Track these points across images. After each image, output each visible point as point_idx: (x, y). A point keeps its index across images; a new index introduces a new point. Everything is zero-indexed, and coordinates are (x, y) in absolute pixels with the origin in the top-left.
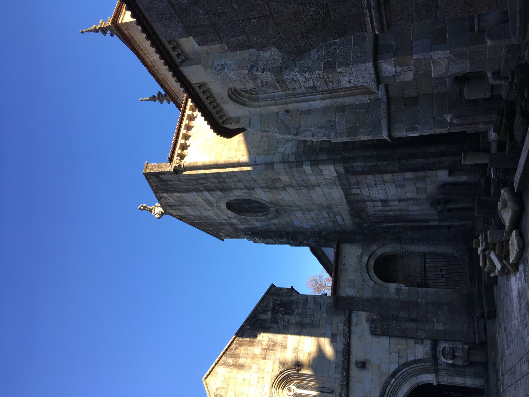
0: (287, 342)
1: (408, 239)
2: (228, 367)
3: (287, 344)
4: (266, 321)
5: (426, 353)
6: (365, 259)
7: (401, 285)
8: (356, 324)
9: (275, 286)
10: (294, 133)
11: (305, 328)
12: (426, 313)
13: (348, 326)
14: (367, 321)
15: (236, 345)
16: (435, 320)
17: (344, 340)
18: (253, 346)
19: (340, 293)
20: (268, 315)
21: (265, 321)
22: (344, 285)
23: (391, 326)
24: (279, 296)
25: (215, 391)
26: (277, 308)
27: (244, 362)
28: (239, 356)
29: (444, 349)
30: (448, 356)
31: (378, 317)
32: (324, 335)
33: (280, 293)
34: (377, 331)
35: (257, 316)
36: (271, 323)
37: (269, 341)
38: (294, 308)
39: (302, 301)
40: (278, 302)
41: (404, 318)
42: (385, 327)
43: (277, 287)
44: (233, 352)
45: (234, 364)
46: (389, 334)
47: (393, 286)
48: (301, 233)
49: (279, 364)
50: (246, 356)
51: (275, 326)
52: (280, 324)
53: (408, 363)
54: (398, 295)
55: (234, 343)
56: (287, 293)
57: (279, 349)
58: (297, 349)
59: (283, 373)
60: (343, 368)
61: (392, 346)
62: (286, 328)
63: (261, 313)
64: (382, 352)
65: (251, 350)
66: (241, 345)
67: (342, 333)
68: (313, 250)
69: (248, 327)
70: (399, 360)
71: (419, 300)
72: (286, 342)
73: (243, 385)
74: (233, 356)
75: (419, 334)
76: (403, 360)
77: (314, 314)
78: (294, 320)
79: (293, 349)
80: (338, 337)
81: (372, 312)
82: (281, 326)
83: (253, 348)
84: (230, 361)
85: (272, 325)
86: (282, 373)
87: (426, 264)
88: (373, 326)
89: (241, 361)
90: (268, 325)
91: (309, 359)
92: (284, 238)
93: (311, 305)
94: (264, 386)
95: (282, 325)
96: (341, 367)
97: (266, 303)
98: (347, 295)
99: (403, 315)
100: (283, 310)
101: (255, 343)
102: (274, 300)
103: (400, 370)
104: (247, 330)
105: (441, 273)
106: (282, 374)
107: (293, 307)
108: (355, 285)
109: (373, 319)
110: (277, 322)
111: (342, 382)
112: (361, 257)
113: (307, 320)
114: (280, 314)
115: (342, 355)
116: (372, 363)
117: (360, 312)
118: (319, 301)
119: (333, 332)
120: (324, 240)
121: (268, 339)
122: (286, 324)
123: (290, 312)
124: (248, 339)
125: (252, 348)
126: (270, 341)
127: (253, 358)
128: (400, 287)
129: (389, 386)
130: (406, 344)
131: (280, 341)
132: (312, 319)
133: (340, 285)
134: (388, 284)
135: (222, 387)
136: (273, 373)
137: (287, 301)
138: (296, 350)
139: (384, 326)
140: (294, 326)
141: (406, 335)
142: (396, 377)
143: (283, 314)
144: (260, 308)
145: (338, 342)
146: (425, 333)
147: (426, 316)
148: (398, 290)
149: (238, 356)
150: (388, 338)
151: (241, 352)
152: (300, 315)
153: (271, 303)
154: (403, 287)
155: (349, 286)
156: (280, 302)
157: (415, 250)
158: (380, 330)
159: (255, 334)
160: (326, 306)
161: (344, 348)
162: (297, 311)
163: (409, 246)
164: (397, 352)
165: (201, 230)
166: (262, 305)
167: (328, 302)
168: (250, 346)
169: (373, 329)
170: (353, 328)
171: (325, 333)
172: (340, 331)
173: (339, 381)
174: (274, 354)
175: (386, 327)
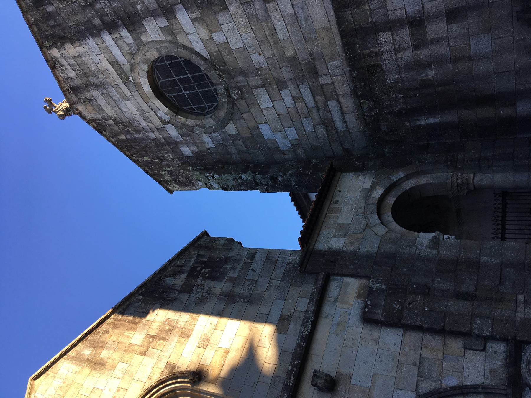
0: (194, 326)
2: (78, 363)
5: (493, 372)
6: (379, 192)
8: (335, 301)
9: (208, 235)
11: (235, 303)
12: (497, 282)
13: (316, 302)
14: (359, 296)
15: (108, 327)
16: (521, 298)
17: (303, 328)
18: (135, 329)
21: (171, 288)
23: (409, 304)
26: (199, 269)
31: (384, 287)
32: (264, 319)
33: (212, 246)
34: (375, 313)
36: (180, 292)
37: (164, 323)
39: (245, 259)
41: (443, 291)
42: (395, 306)
43: (211, 236)
44: (99, 337)
45: (90, 359)
46: (402, 321)
47: (425, 238)
49: (164, 367)
51: (184, 297)
53: (442, 390)
54: (438, 249)
55: (107, 323)
56: (224, 245)
57: (176, 339)
59: (164, 385)
60: (286, 386)
61: (407, 349)
63: (170, 276)
64: (381, 361)
65: (128, 337)
66: (115, 326)
67: (302, 315)
68: (296, 200)
69: (141, 297)
71: (483, 259)
72: (193, 325)
75: (476, 326)
77: (260, 279)
79: (200, 340)
86: (162, 383)
87: (507, 213)
88: (369, 303)
89: (104, 354)
91: (223, 362)
93: (257, 265)
95: (197, 296)
96: (281, 385)
97: (183, 261)
98: (329, 248)
101: (141, 325)
102: (199, 256)
106: (161, 386)
107: (227, 268)
108: (348, 232)
109: (372, 289)
113: (243, 290)
116: (353, 382)
117: (347, 279)
118: (274, 259)
119: (285, 313)
121: (163, 319)
122: (204, 294)
123: (218, 275)
124: (131, 318)
126: (166, 323)
130: (441, 348)
131: (183, 324)
133: (320, 232)
137: (220, 258)
138: (205, 343)
139: (394, 305)
140: (216, 299)
141: (444, 327)
146: (492, 323)
148: (435, 243)
150: (400, 332)
151: (112, 338)
152: (234, 281)
153: (193, 260)
156: (206, 260)
157: (484, 182)
158: (383, 312)
161: (299, 345)
162: (231, 274)
164: (418, 363)
165: (134, 161)
167: (291, 260)
168: (129, 330)
169: (366, 310)
170: (327, 308)
171: (268, 315)
172: (299, 311)
174: (162, 347)
175: (398, 306)
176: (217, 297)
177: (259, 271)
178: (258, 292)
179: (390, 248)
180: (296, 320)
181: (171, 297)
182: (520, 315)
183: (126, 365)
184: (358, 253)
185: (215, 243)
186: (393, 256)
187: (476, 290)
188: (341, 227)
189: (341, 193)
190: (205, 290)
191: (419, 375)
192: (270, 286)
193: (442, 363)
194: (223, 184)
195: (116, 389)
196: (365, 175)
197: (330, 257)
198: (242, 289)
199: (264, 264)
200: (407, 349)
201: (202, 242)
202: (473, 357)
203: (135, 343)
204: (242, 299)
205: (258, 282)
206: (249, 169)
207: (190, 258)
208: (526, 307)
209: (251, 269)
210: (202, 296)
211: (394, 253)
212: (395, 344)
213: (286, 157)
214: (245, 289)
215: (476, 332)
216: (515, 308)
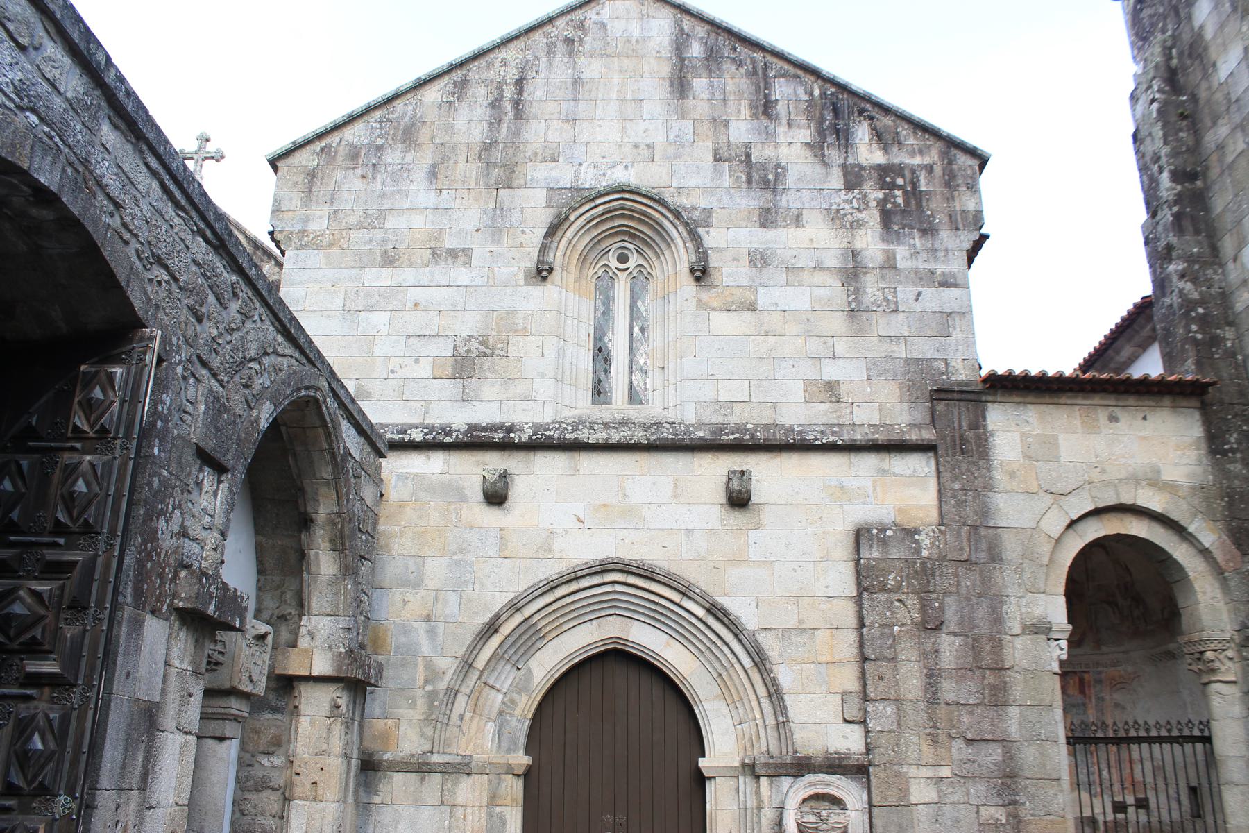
2: (675, 46)
6: (1155, 502)
7: (1064, 644)
9: (982, 167)
11: (843, 285)
12: (969, 736)
13: (872, 440)
14: (900, 511)
15: (749, 61)
17: (821, 428)
18: (755, 116)
19: (996, 405)
20: (867, 153)
23: (899, 601)
24: (947, 185)
25: (595, 18)
26: (900, 181)
27: (697, 93)
28: (713, 75)
29: (836, 802)
30: (812, 818)
31: (925, 553)
33: (958, 186)
34: (871, 547)
36: (844, 167)
37: (778, 166)
38: (912, 242)
42: (891, 577)
44: (726, 55)
45: (686, 62)
46: (865, 593)
47: (1055, 610)
48: (1215, 250)
49: (703, 206)
50: (718, 96)
52: (843, 197)
53: (768, 666)
54: (1025, 630)
57: (754, 203)
58: (765, 264)
60: (721, 430)
61: (823, 607)
63: (874, 129)
65: (739, 111)
67: (845, 420)
69: (817, 93)
70: (772, 633)
71: (1014, 711)
72: (785, 224)
73: (622, 100)
74: (712, 57)
75: (881, 708)
78: (865, 246)
79: (761, 250)
81: (943, 528)
82: (837, 200)
83: (748, 117)
84: (696, 50)
88: (889, 533)
89: (700, 84)
90: (834, 156)
92: (1179, 188)
94: (626, 167)
96: (720, 420)
97: (911, 141)
99: (949, 648)
102: (930, 169)
103: (736, 636)
104: (805, 90)
105: (1130, 800)
107: (914, 239)
108: (1038, 461)
111: (668, 426)
112: (1155, 482)
114: (880, 195)
118: (951, 330)
119: (844, 389)
120: (1199, 336)
122: (849, 216)
123: (896, 228)
125: (745, 112)
126: (779, 171)
127: (714, 119)
128: (1056, 640)
129: (676, 597)
130: (837, 658)
131: (784, 203)
132: (881, 309)
133: (1029, 406)
134: (1062, 589)
135: (608, 39)
136: (671, 190)
137: (932, 215)
139: (893, 575)
140: (845, 245)
142: (711, 621)
143: (882, 204)
147: (955, 738)
148: (1041, 629)
149: (714, 72)
151: (730, 81)
152: (889, 264)
153: (917, 160)
154: (1058, 651)
156: (923, 188)
158: (874, 560)
159: (796, 116)
161: (789, 430)
162: (901, 253)
163: (1232, 678)
164: (803, 627)
166: (904, 129)
168: (753, 107)
169: (875, 531)
170: (869, 462)
171: (834, 357)
172: (852, 413)
173: (671, 415)
175: (893, 583)
176: (849, 246)
177: (918, 307)
179: (1011, 548)
180: (835, 412)
181: (829, 154)
182: (913, 771)
183: (690, 137)
184: (990, 491)
185: (965, 189)
186: (995, 558)
187: (947, 704)
188: (1052, 442)
189: (1140, 422)
190: (860, 216)
192: (892, 341)
193: (812, 662)
194: (1143, 133)
195: (649, 140)
196: (1200, 462)
198: (875, 289)
200: (823, 607)
201: (963, 160)
203: (731, 130)
204: (854, 297)
205: (894, 315)
207: (921, 152)
208: (929, 780)
209: (920, 289)
211: (1002, 559)
212: (827, 587)
213: (1231, 266)
214: (877, 293)
216: (924, 764)
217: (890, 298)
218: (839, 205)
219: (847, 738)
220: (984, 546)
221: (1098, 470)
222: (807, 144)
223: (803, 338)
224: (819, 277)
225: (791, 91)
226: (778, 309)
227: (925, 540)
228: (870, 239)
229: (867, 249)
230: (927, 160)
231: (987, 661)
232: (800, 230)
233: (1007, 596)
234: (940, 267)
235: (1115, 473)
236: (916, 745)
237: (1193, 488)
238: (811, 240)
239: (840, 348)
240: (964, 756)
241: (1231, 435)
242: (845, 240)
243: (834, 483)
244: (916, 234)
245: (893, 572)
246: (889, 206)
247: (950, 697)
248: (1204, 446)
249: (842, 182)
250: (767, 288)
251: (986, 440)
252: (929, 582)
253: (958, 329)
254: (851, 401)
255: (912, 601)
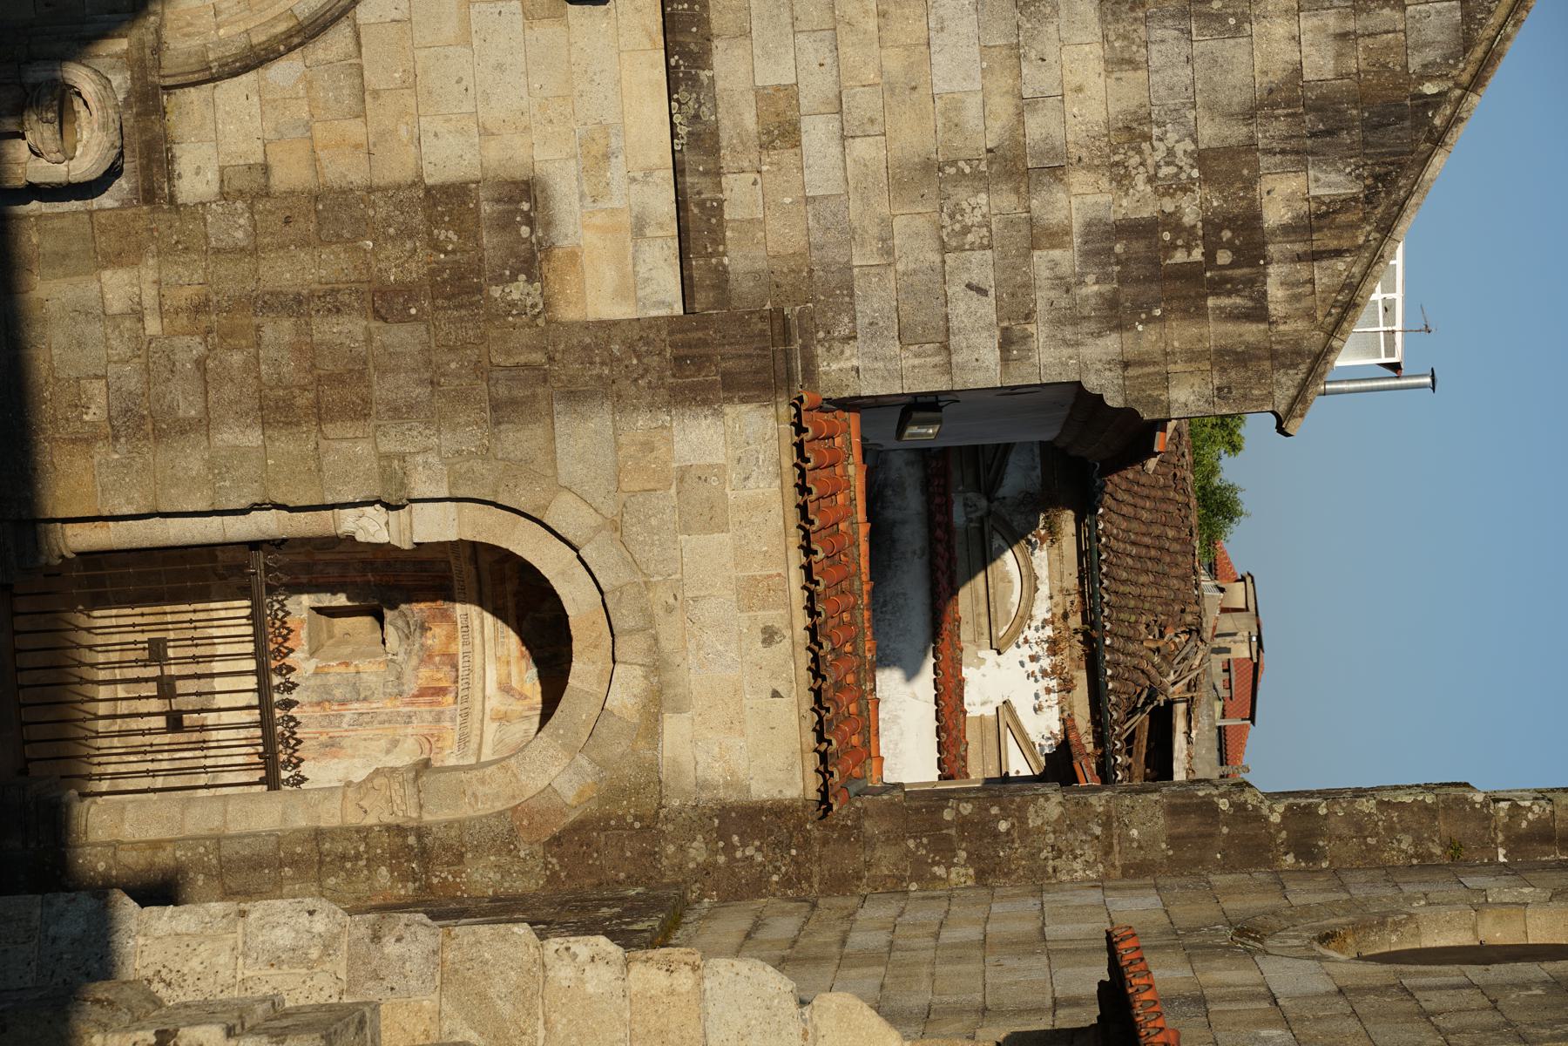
0: (1105, 37)
1: (349, 865)
3: (1103, 20)
4: (1297, 153)
10: (399, 940)
11: (989, 151)
12: (210, 364)
14: (573, 256)
21: (1298, 155)
22: (751, 483)
24: (1221, 352)
26: (1224, 257)
31: (496, 292)
33: (1223, 370)
34: (498, 201)
35: (1376, 178)
36: (1250, 146)
37: (1244, 18)
38: (1090, 279)
40: (1225, 301)
42: (451, 234)
51: (1210, 133)
52: (1179, 149)
61: (403, 131)
62: (1128, 128)
63: (1346, 203)
64: (459, 81)
69: (1430, 89)
70: (352, 47)
71: (254, 438)
72: (1112, 37)
75: (242, 221)
76: (331, 56)
77: (937, 258)
78: (1075, 190)
80: (750, 122)
82: (1172, 137)
85: (1237, 133)
88: (525, 231)
98: (718, 414)
100: (1176, 247)
102: (1259, 313)
104: (1434, 63)
107: (1097, 282)
110: (1201, 158)
112: (657, 703)
114: (1190, 216)
115: (708, 21)
119: (788, 156)
122: (1135, 160)
126: (1232, 21)
130: (321, 154)
131: (1158, 34)
132: (946, 220)
134: (469, 536)
137: (1151, 320)
143: (1171, 221)
144: (1361, 240)
145: (751, 97)
146: (206, 237)
152: (1040, 236)
155: (714, 482)
158: (477, 205)
159: (1366, 48)
160: (862, 322)
164: (368, 98)
167: (848, 353)
169: (525, 206)
171: (843, 138)
177: (956, 289)
178: (919, 209)
179: (520, 440)
180: (742, 142)
181: (1277, 118)
185: (1216, 382)
186: (502, 411)
187: (258, 328)
188: (712, 518)
190: (1140, 180)
191: (360, 68)
196: (702, 785)
197: (701, 379)
198: (985, 209)
199: (947, 320)
202: (243, 147)
204: (967, 170)
205: (936, 245)
206: (1284, 834)
208: (137, 299)
209: (992, 292)
210: (1140, 152)
211: (500, 423)
212: (436, 135)
214: (977, 212)
215: (239, 205)
217: (970, 238)
218: (1161, 140)
219: (197, 174)
220: (519, 393)
221: (671, 601)
222: (1298, 71)
223: (877, 80)
224: (1003, 107)
225: (1430, 34)
226: (932, 34)
227: (518, 290)
228: (1090, 199)
229: (1067, 191)
230: (1276, 308)
231: (331, 394)
232: (1100, 67)
233: (438, 430)
234: (1039, 331)
235: (669, 632)
236: (188, 281)
237: (654, 767)
238: (1079, 89)
239: (861, 148)
240: (180, 356)
241: (758, 849)
242: (1084, 153)
243: (614, 142)
244: (1106, 288)
245: (459, 238)
246: (1167, 236)
247: (268, 333)
248: (732, 797)
249: (1214, 144)
250: (972, 11)
251: (705, 402)
252: (448, 298)
253: (917, 362)
254: (765, 168)
255: (415, 271)
